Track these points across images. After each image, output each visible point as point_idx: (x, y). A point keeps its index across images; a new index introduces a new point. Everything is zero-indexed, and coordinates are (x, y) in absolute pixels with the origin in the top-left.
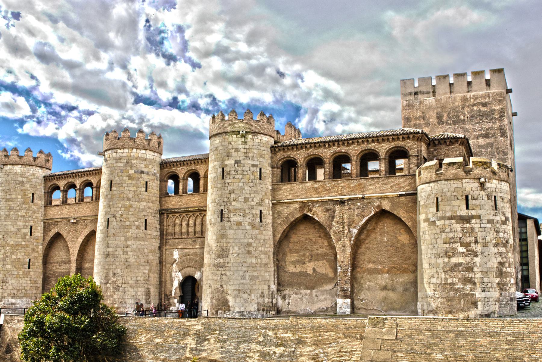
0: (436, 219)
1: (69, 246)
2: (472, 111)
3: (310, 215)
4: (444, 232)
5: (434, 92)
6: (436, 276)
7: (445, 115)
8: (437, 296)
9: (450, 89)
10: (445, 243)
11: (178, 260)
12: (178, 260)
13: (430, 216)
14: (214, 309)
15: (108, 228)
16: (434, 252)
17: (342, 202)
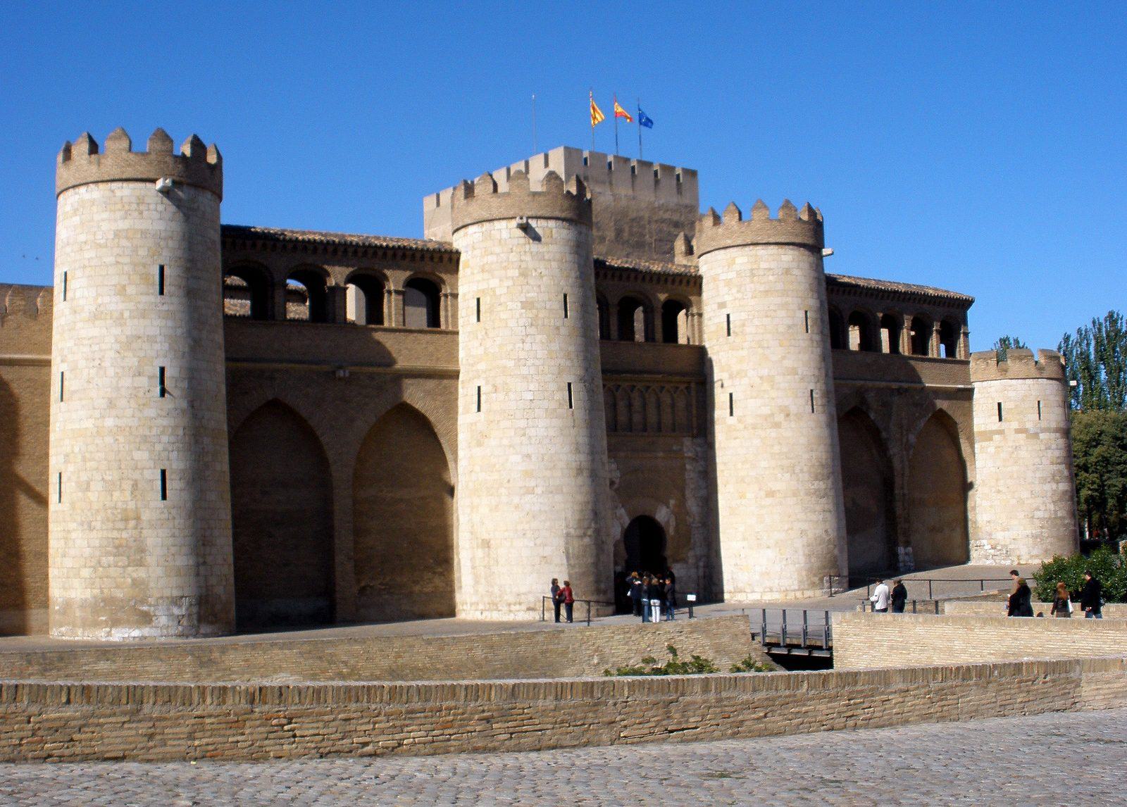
0: (1039, 431)
1: (324, 439)
2: (661, 231)
3: (864, 408)
4: (1049, 448)
5: (611, 183)
6: (1042, 508)
7: (627, 229)
8: (1046, 535)
9: (633, 182)
10: (1052, 463)
11: (617, 481)
12: (617, 481)
13: (1029, 425)
14: (815, 575)
15: (571, 407)
16: (1038, 475)
17: (899, 391)
